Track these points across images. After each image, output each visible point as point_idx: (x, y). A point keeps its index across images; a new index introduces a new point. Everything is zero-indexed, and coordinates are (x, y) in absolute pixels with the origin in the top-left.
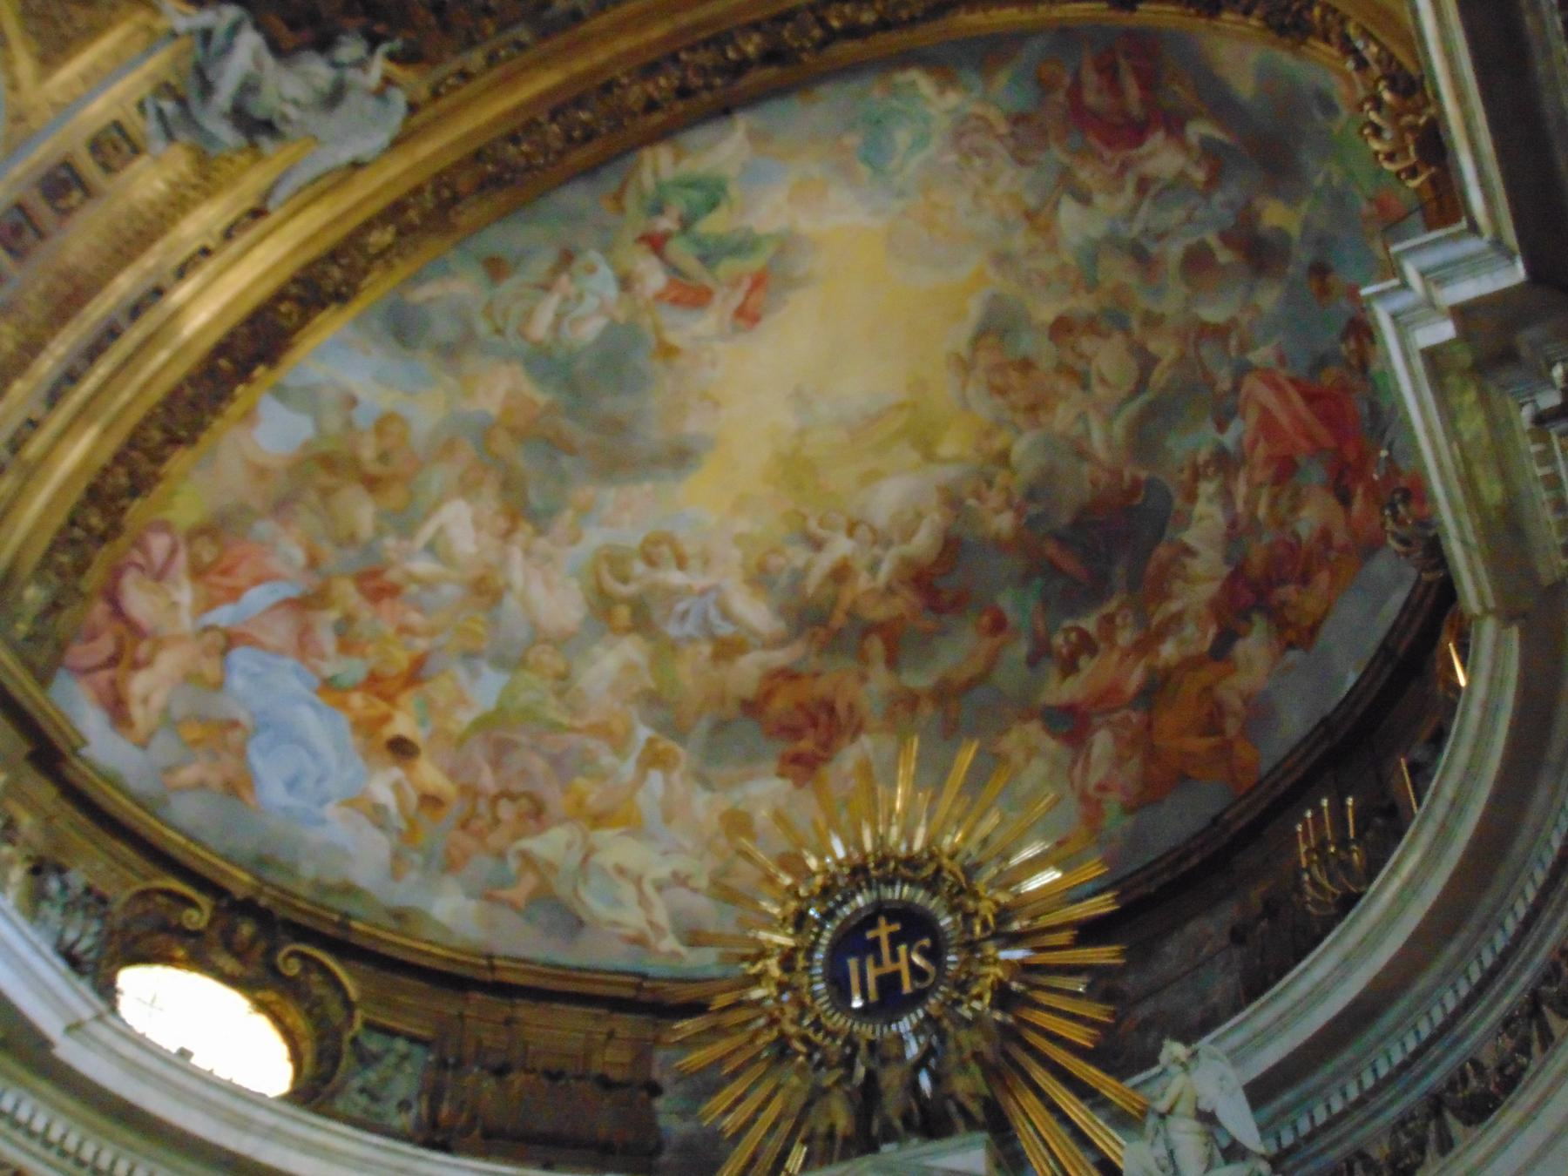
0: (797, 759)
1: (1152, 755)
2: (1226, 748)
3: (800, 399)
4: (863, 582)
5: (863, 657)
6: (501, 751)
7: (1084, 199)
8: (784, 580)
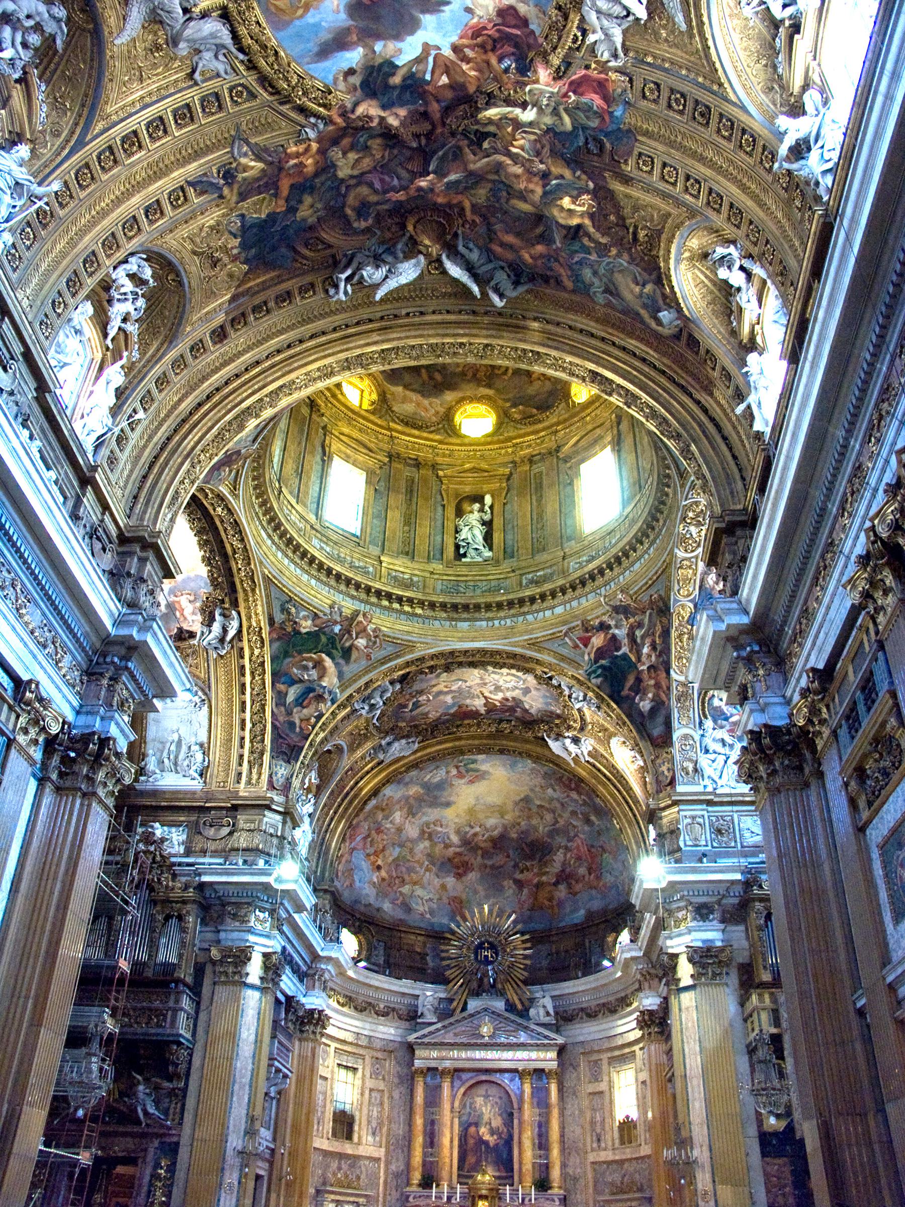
1: (536, 899)
3: (477, 799)
6: (397, 866)
7: (555, 790)
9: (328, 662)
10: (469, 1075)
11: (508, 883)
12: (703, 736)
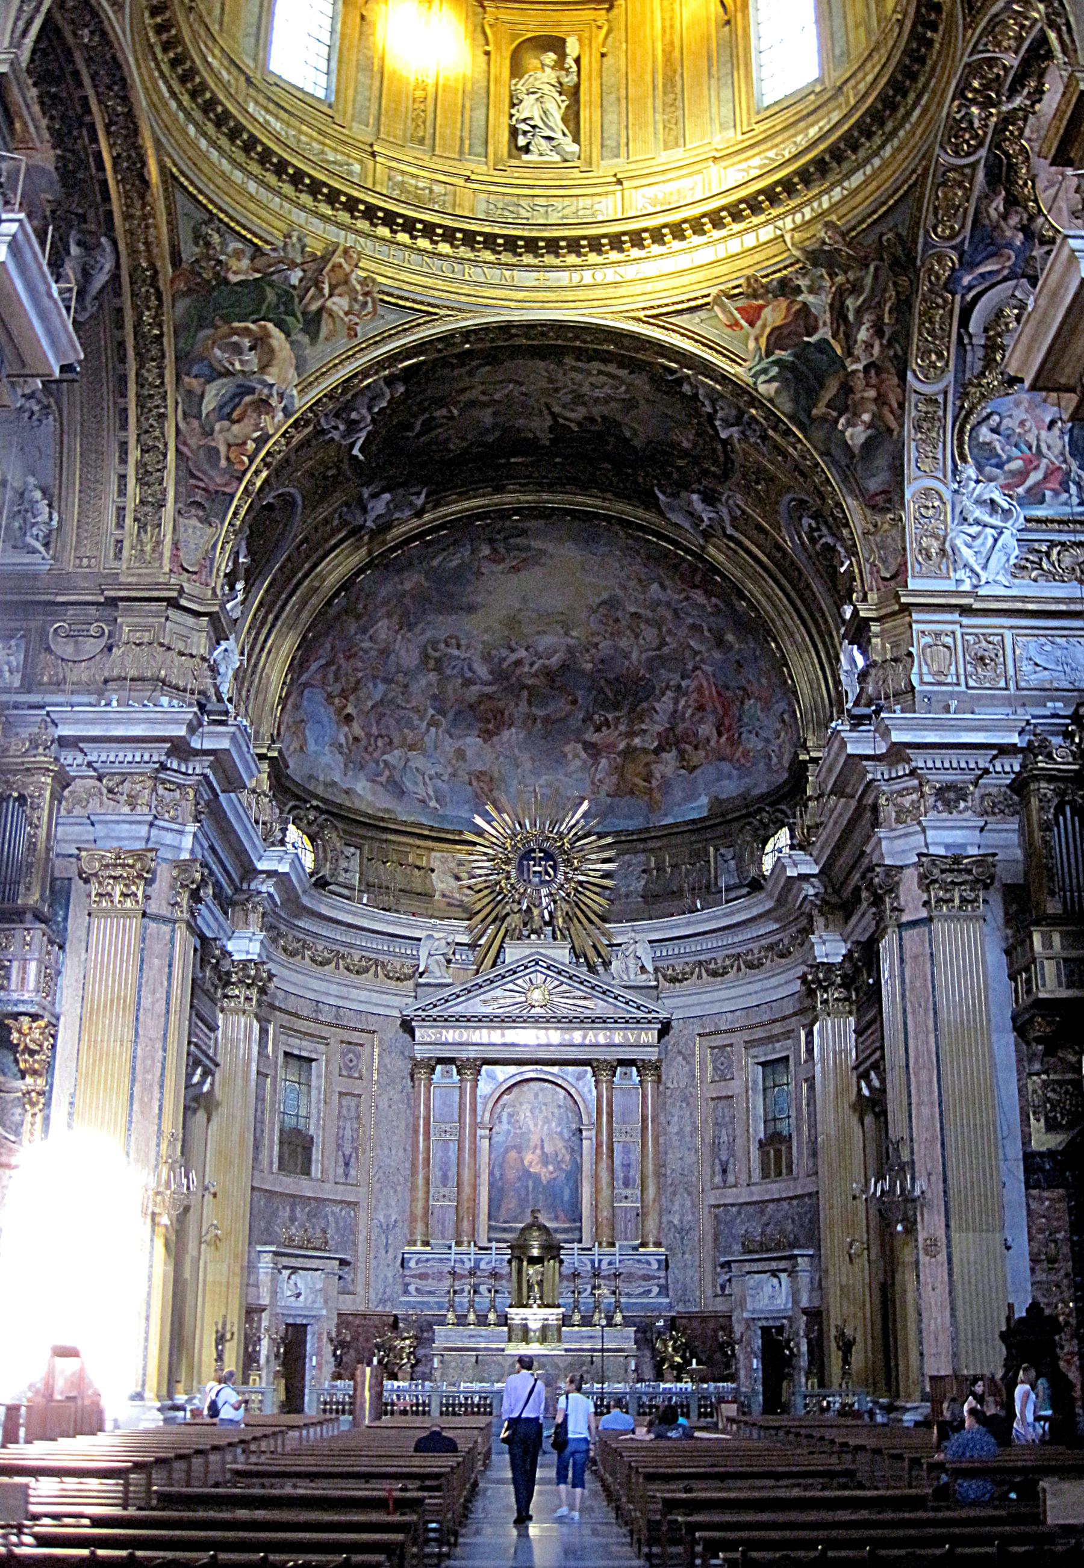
0: (487, 731)
1: (622, 776)
2: (651, 789)
4: (526, 669)
5: (518, 696)
7: (663, 587)
8: (496, 660)
9: (277, 338)
10: (512, 1069)
11: (573, 749)
12: (956, 492)
